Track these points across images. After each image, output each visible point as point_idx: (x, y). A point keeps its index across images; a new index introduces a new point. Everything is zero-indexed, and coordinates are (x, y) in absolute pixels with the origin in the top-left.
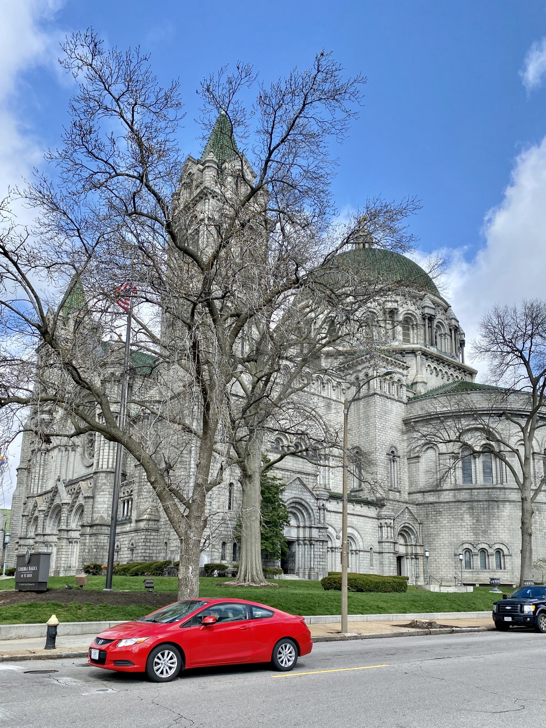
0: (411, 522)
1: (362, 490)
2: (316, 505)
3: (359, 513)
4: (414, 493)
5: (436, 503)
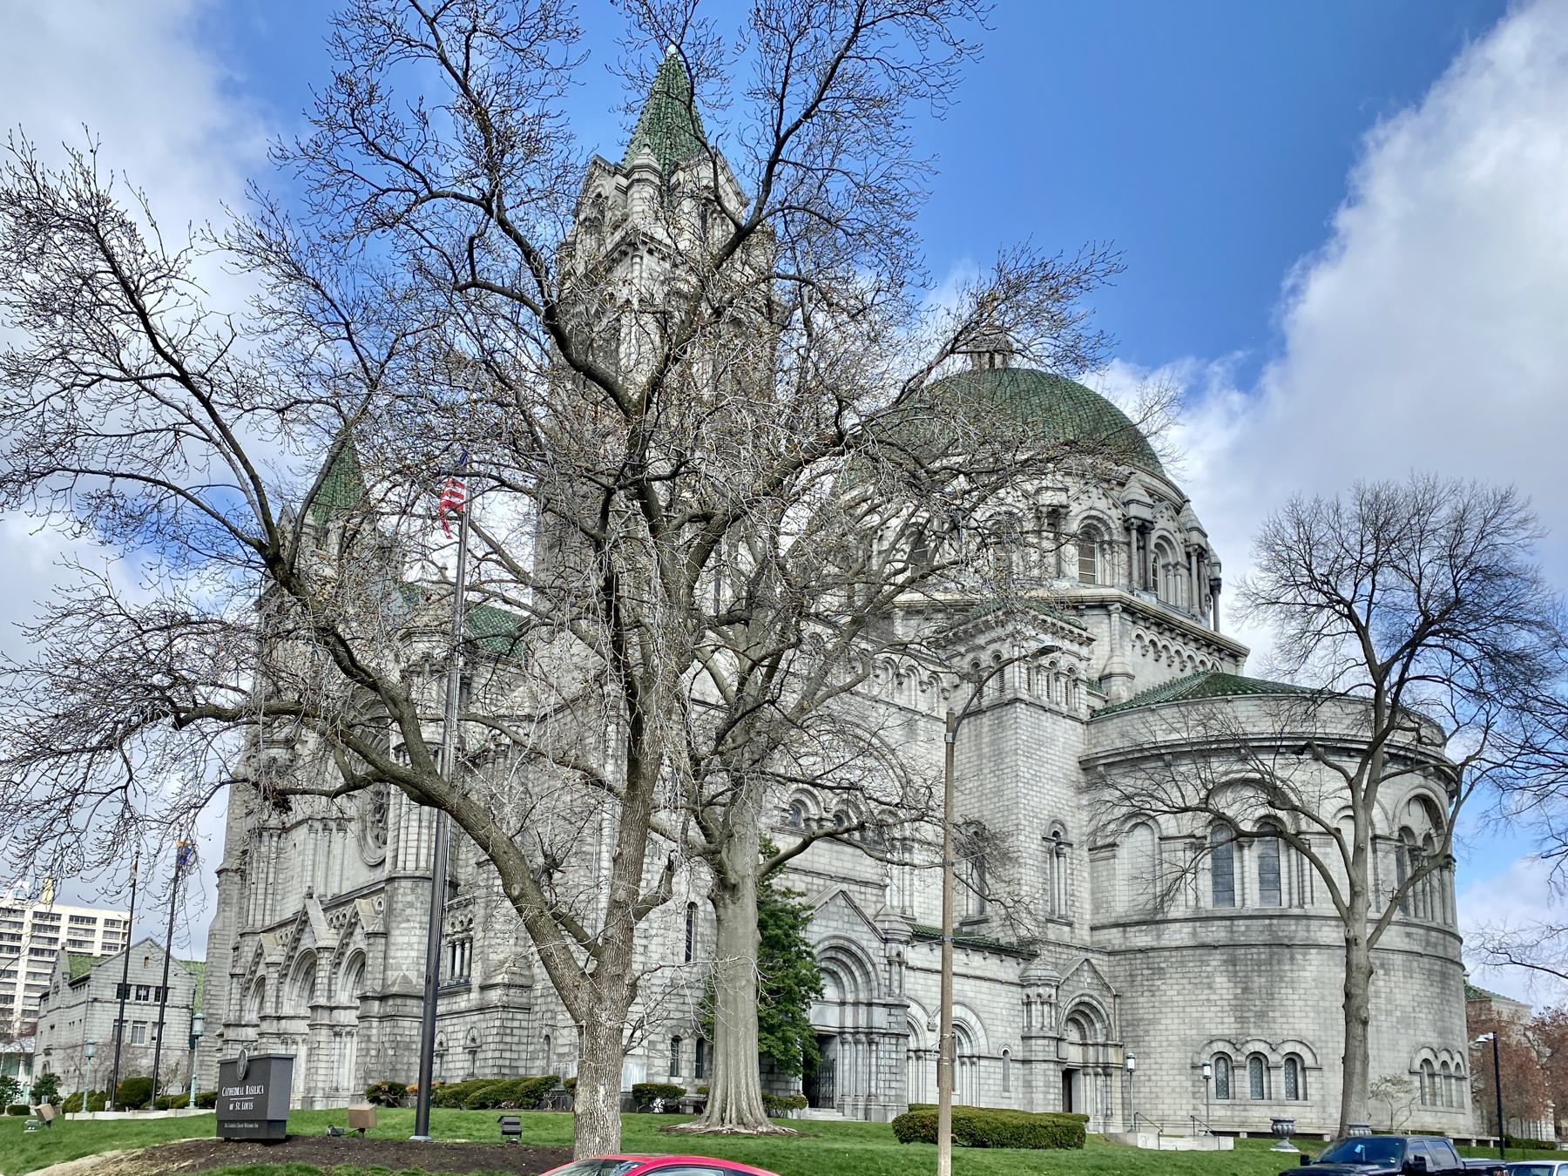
0: (1095, 994)
1: (986, 921)
3: (979, 973)
4: (1104, 927)
5: (1153, 949)
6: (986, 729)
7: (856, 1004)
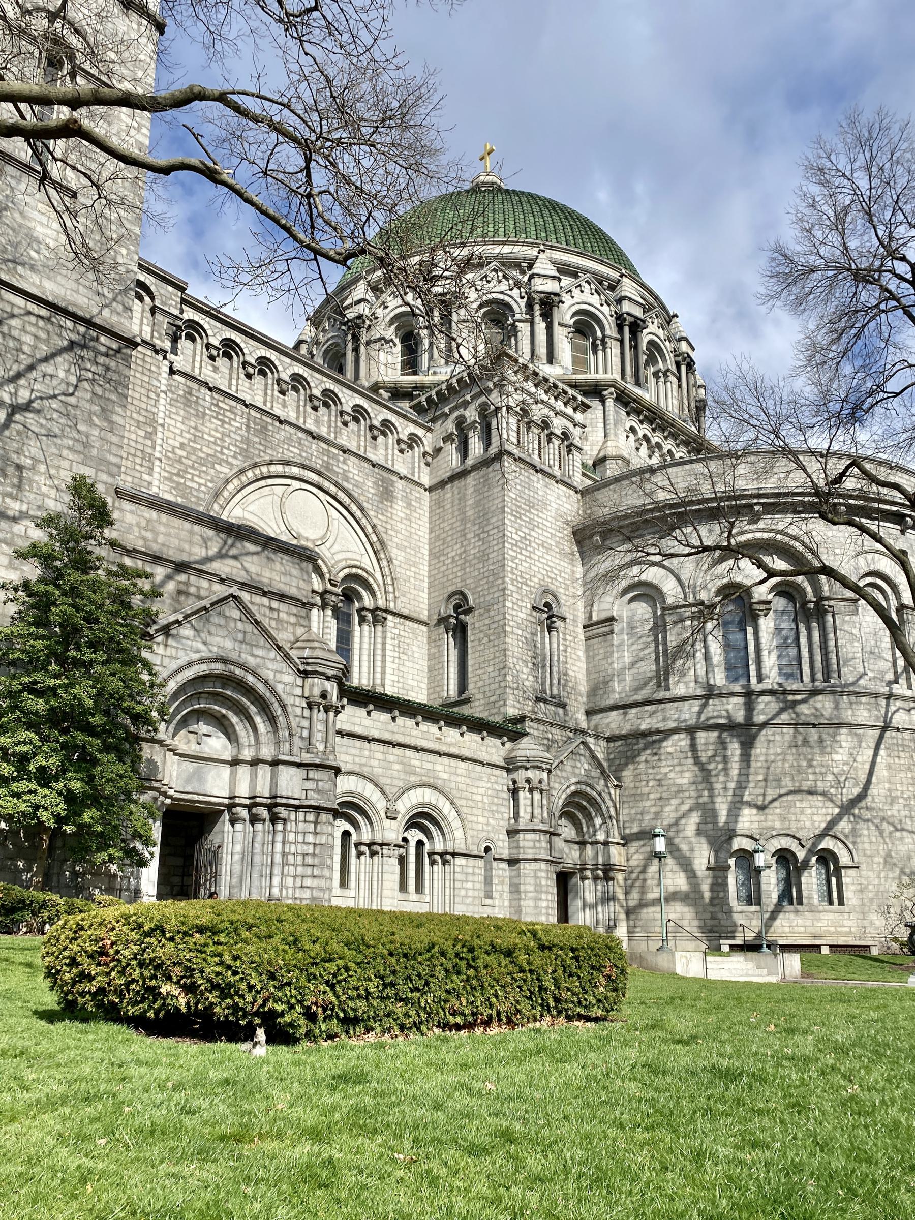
1: (467, 701)
2: (298, 691)
6: (470, 490)
7: (255, 763)
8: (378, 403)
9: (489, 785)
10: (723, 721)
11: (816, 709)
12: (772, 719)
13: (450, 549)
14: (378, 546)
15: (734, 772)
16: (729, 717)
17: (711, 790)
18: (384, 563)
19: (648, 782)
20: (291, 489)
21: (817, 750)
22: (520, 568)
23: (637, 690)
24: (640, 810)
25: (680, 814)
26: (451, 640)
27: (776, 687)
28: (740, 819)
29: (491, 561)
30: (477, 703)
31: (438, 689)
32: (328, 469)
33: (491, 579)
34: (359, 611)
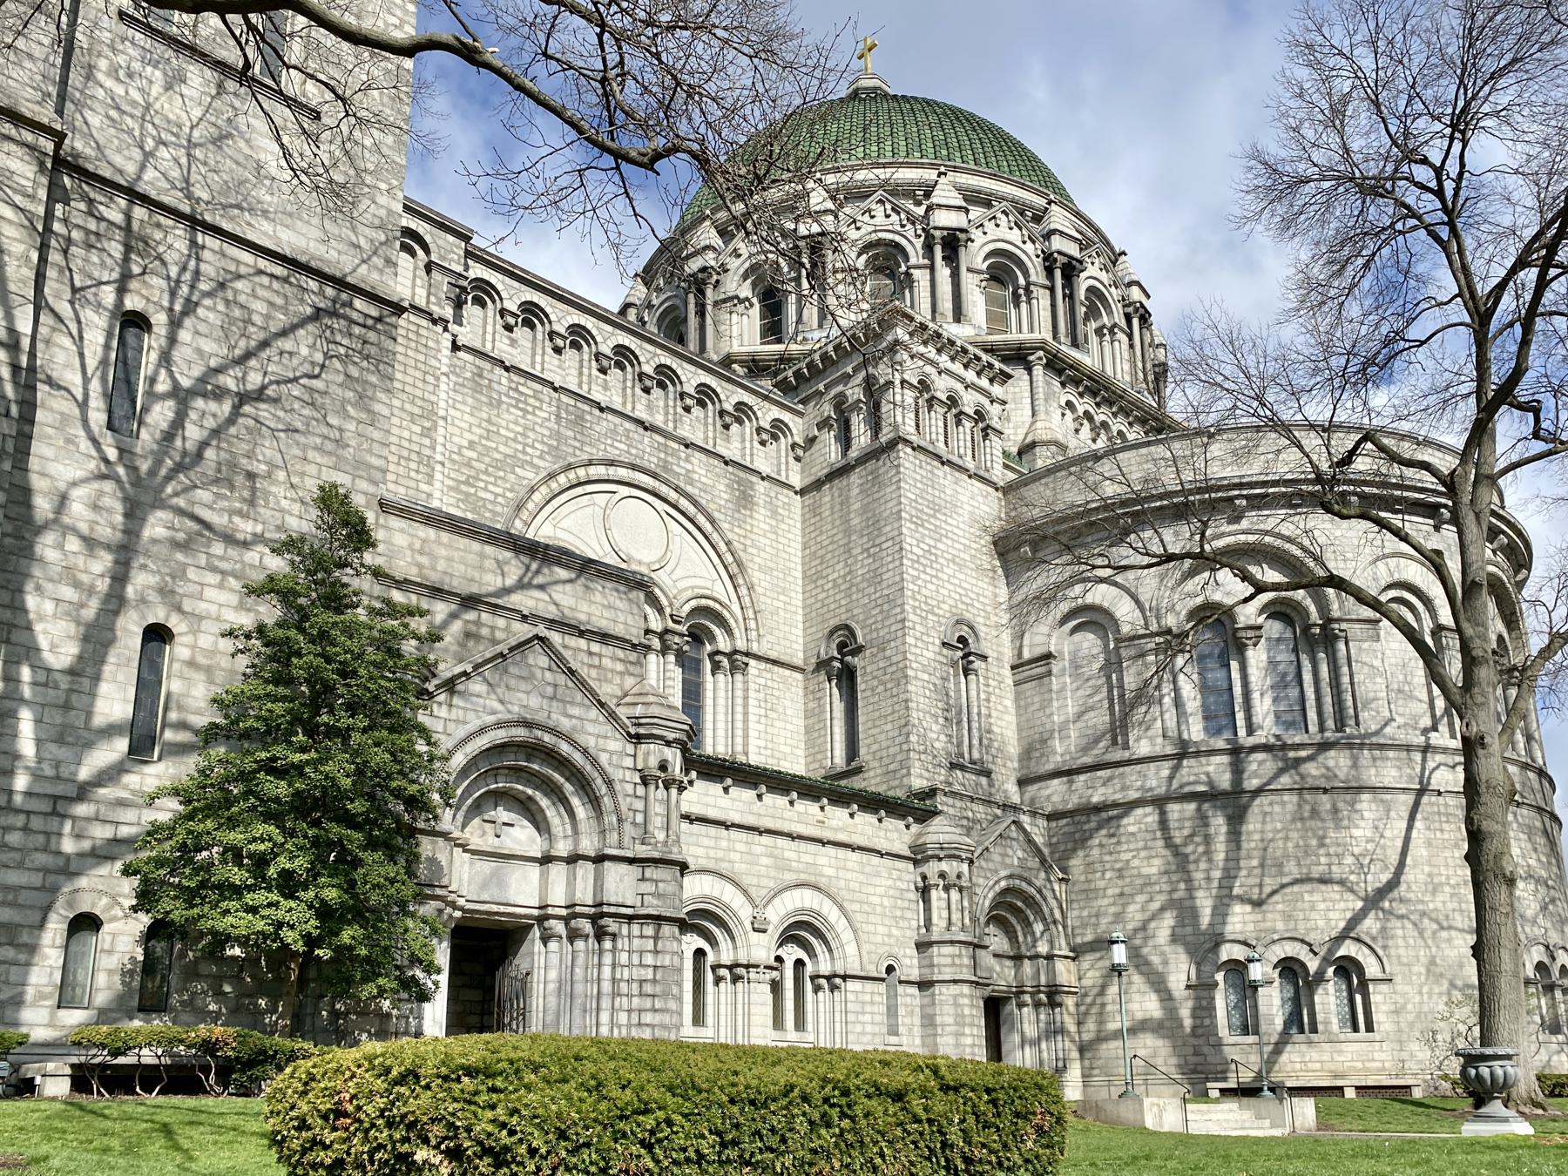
1: (859, 770)
2: (629, 762)
3: (842, 837)
7: (573, 859)
8: (729, 380)
9: (890, 882)
10: (1202, 788)
11: (1328, 769)
12: (1268, 783)
13: (830, 570)
14: (734, 569)
15: (1220, 856)
16: (1210, 783)
17: (1189, 881)
18: (743, 591)
19: (1103, 873)
20: (617, 497)
21: (1330, 824)
22: (924, 591)
23: (1085, 750)
24: (1094, 911)
25: (1149, 914)
26: (835, 690)
27: (1272, 740)
28: (1230, 919)
29: (884, 584)
30: (872, 773)
31: (819, 756)
32: (665, 468)
33: (886, 607)
34: (712, 655)
